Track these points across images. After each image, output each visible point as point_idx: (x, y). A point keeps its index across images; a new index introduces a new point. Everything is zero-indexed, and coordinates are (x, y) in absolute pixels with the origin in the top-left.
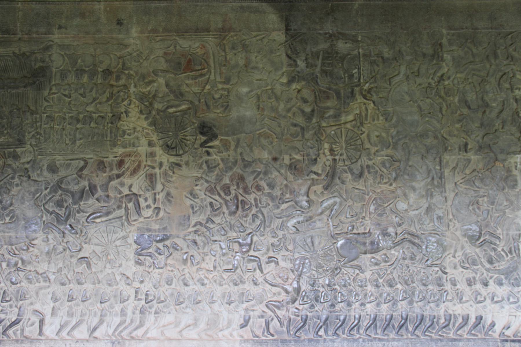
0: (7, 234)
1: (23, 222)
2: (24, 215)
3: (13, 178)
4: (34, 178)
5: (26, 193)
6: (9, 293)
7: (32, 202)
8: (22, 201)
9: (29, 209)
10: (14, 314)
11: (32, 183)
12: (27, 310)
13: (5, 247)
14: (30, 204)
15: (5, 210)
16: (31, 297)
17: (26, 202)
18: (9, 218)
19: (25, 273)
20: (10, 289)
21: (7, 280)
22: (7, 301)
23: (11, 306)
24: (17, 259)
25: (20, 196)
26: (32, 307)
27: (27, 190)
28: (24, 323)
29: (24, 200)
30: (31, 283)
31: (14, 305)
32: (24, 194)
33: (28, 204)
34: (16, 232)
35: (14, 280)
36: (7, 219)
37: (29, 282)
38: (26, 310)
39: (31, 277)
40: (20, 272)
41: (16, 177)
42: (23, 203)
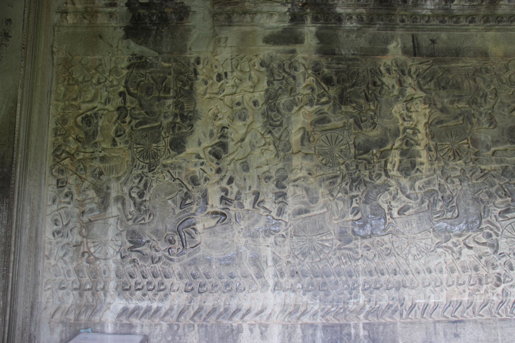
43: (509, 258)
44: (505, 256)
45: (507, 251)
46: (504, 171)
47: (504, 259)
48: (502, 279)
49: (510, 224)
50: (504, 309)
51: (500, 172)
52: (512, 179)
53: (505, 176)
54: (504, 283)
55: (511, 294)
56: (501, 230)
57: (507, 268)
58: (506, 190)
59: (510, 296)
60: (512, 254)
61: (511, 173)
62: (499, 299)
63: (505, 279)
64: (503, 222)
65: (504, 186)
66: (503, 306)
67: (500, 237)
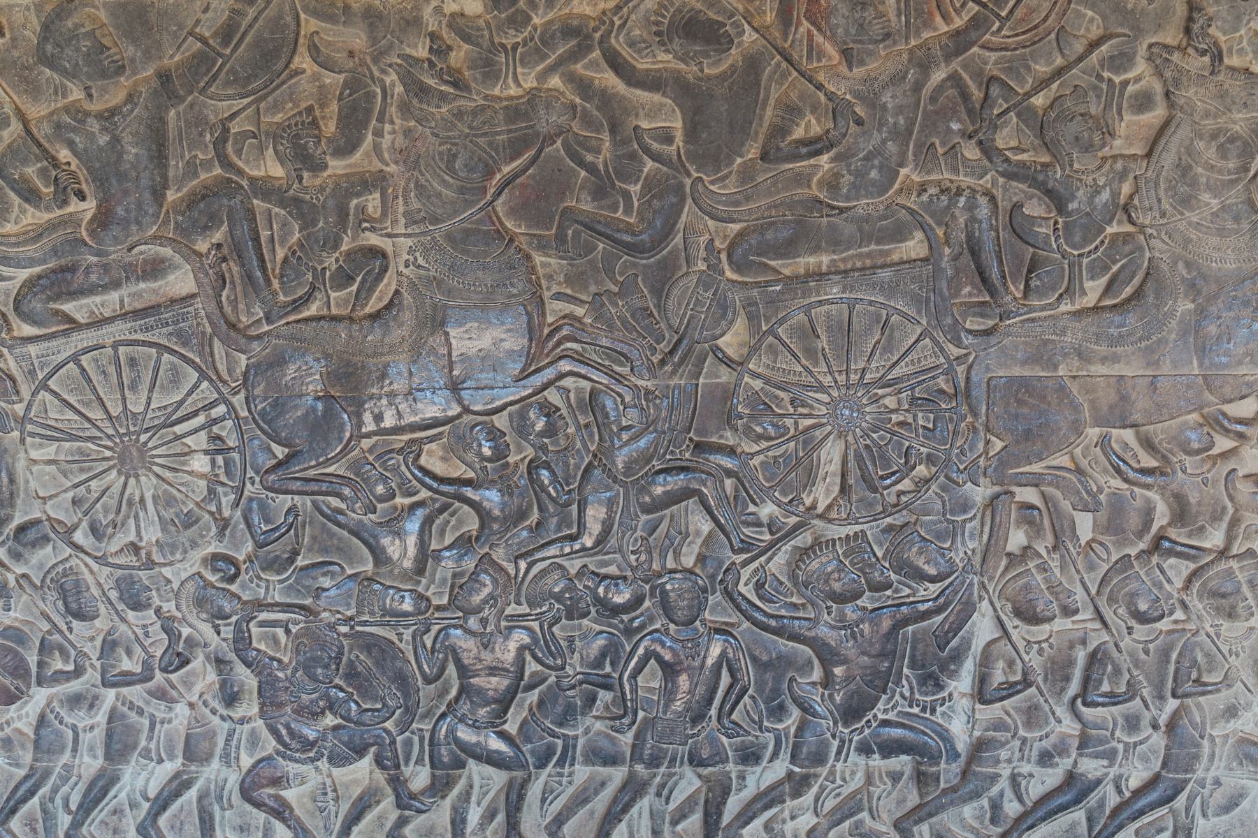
0: (1099, 369)
1: (1185, 306)
2: (1188, 265)
3: (1121, 61)
4: (1234, 61)
5: (1201, 145)
6: (1124, 661)
7: (1234, 196)
8: (1183, 189)
9: (1221, 232)
10: (1145, 759)
11: (1235, 86)
12: (1212, 739)
13: (1093, 433)
14: (1224, 208)
15: (1086, 241)
16: (1227, 681)
17: (1206, 197)
18: (1104, 280)
19: (1192, 566)
20: (1126, 642)
21: (1112, 600)
22: (1114, 699)
23: (1132, 724)
24: (1153, 495)
25: (1168, 159)
26: (1233, 725)
27: (1209, 124)
28: (1191, 800)
29: (1193, 183)
30: (1231, 615)
31: (1147, 717)
32: (1190, 151)
33: (1215, 203)
34: (1151, 356)
35: (1143, 606)
36: (1093, 289)
37: (1218, 609)
38: (1206, 743)
39: (1229, 587)
40: (1172, 561)
41: (1142, 50)
42: (1186, 202)
43: (69, 551)
44: (46, 539)
45: (59, 511)
46: (46, 27)
47: (45, 555)
48: (32, 659)
49: (75, 358)
50: (39, 815)
51: (31, 35)
52: (96, 86)
53: (51, 62)
54: (39, 684)
55: (76, 740)
56: (26, 393)
57: (51, 604)
58: (64, 154)
59: (75, 750)
60: (84, 524)
61: (86, 44)
62: (17, 765)
63: (41, 664)
64: (33, 349)
65: (43, 131)
66: (35, 800)
67: (16, 434)
